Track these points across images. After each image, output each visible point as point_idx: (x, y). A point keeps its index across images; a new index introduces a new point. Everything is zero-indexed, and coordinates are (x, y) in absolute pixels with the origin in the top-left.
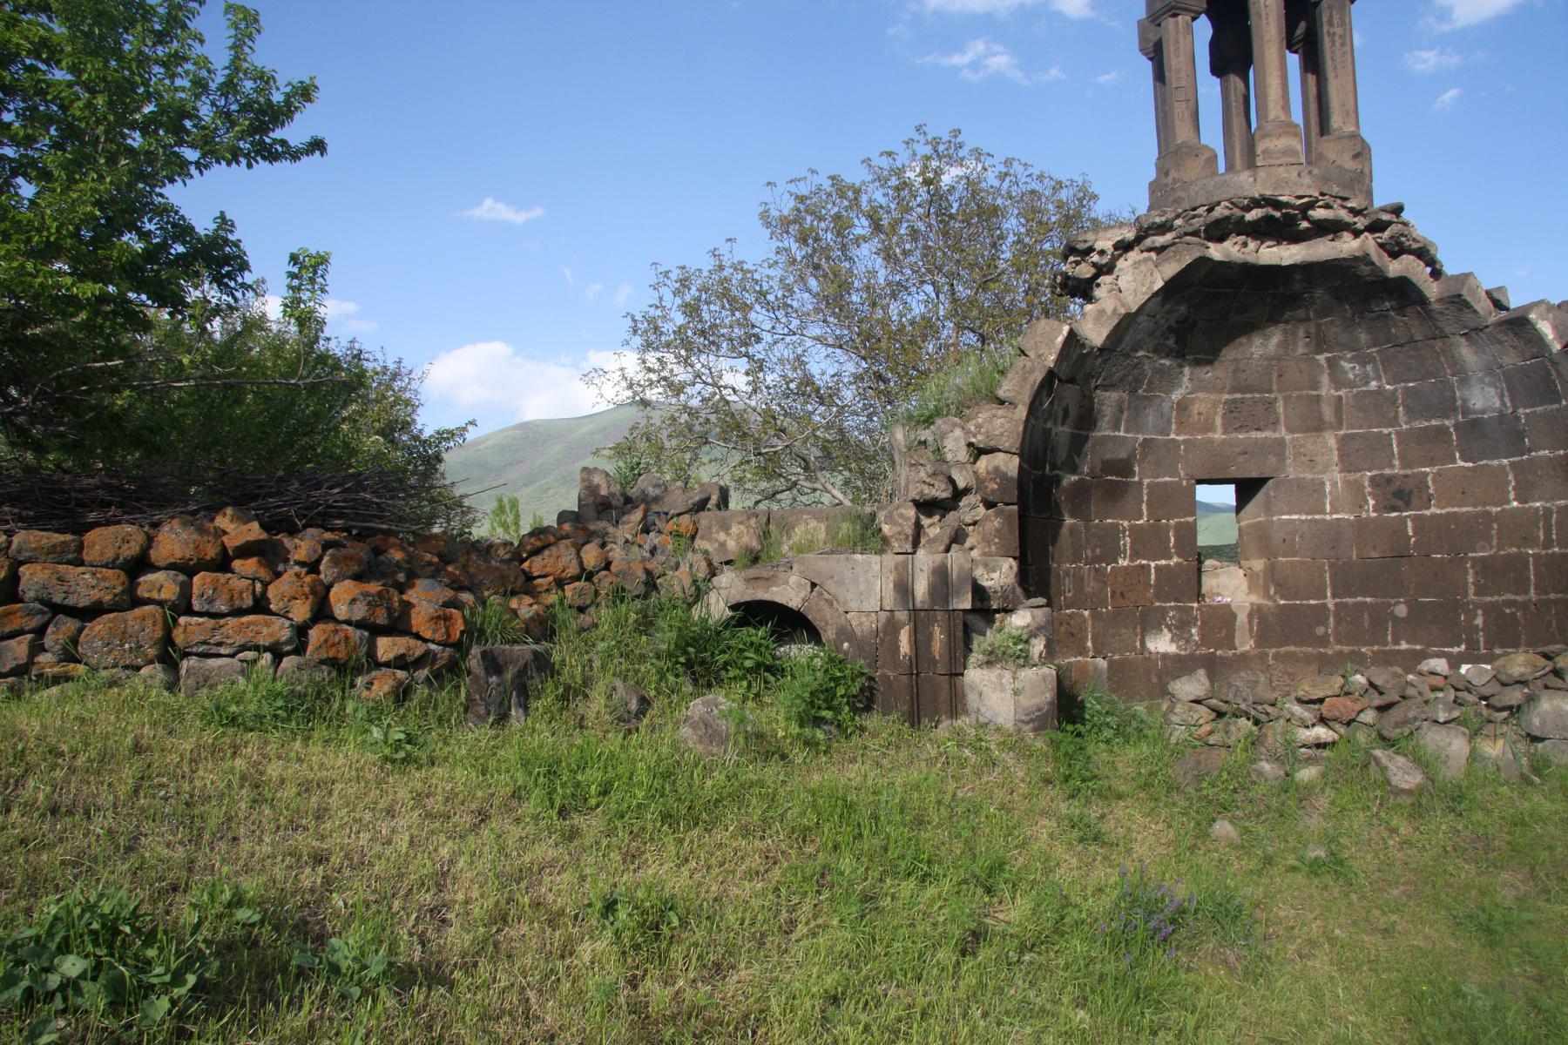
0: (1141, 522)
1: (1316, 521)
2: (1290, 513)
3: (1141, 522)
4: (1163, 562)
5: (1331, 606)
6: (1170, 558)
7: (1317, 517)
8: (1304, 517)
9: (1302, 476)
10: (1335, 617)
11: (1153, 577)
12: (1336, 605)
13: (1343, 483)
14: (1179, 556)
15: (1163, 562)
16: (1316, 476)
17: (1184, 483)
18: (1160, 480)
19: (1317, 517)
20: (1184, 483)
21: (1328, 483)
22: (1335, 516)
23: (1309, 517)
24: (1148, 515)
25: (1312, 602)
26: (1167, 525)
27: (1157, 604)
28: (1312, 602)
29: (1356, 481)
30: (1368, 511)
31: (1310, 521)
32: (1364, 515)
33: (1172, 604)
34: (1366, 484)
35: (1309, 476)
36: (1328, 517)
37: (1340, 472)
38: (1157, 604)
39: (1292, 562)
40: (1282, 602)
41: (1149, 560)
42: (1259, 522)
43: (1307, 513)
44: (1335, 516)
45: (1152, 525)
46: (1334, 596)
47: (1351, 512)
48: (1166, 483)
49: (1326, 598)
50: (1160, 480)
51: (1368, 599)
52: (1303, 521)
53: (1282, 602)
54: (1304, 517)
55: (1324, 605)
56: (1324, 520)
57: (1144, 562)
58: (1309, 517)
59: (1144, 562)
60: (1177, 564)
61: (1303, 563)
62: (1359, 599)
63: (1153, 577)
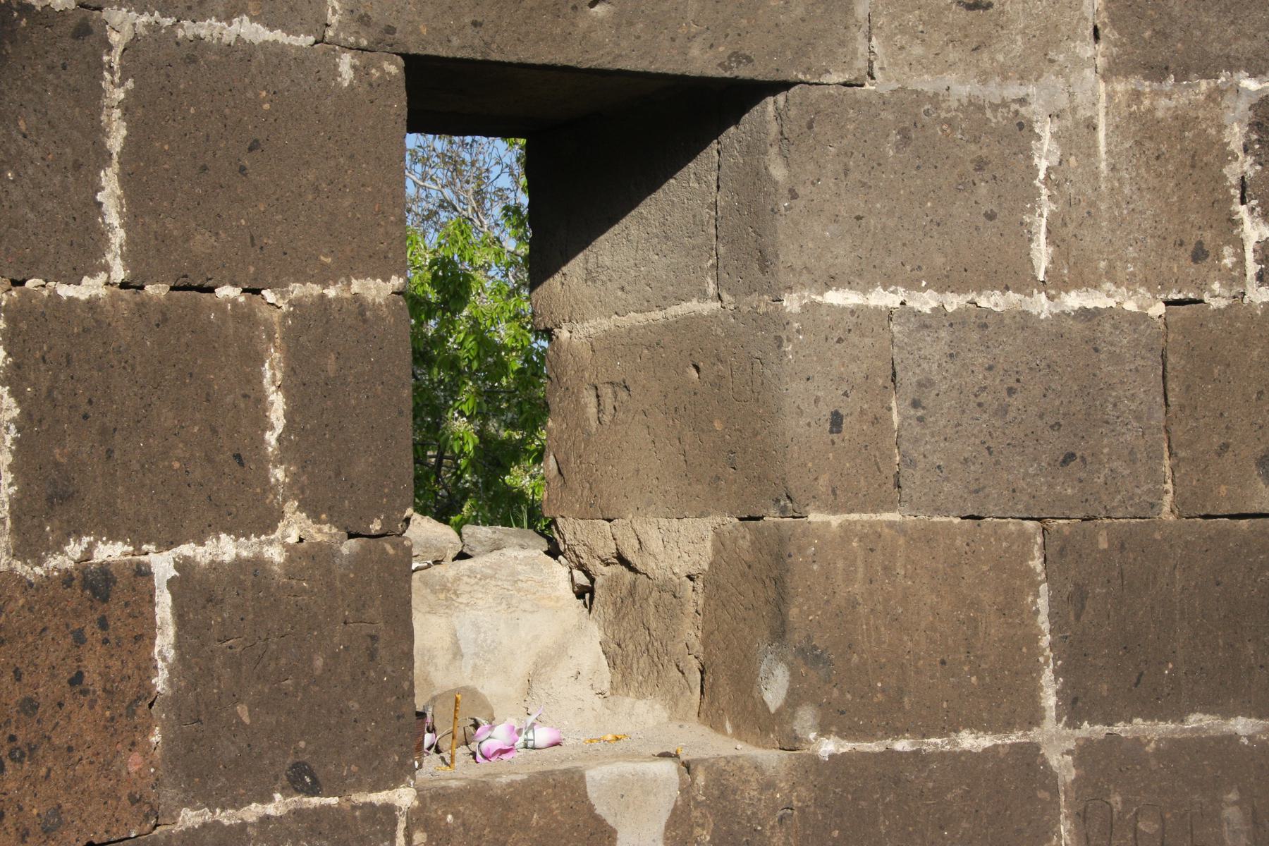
0: (90, 288)
1: (983, 321)
2: (859, 278)
3: (90, 288)
4: (226, 548)
5: (1059, 761)
6: (267, 522)
7: (992, 301)
8: (926, 301)
9: (925, 83)
10: (1082, 817)
11: (165, 643)
12: (1085, 754)
13: (1116, 129)
14: (313, 510)
15: (226, 548)
16: (993, 91)
17: (346, 63)
18: (209, 29)
19: (992, 301)
20: (346, 63)
21: (1046, 129)
22: (1073, 300)
23: (954, 302)
24: (130, 257)
25: (969, 741)
26: (245, 317)
27: (190, 818)
28: (969, 741)
29: (1183, 121)
30: (1235, 277)
31: (956, 321)
32: (1217, 298)
33: (278, 806)
34: (1236, 136)
35: (960, 87)
36: (1040, 305)
37: (1108, 74)
38: (190, 818)
39: (872, 539)
40: (828, 747)
41: (138, 539)
42: (690, 322)
43: (943, 284)
44: (1073, 300)
45: (164, 315)
46: (1073, 709)
47: (1154, 281)
48: (243, 52)
49: (1035, 718)
50: (209, 29)
51: (1242, 726)
52: (924, 323)
53: (828, 747)
54: (926, 301)
55: (1029, 754)
56: (1025, 320)
57: (111, 552)
58: (954, 302)
59: (111, 552)
60: (301, 554)
61: (927, 536)
62: (1197, 721)
63: (165, 643)
